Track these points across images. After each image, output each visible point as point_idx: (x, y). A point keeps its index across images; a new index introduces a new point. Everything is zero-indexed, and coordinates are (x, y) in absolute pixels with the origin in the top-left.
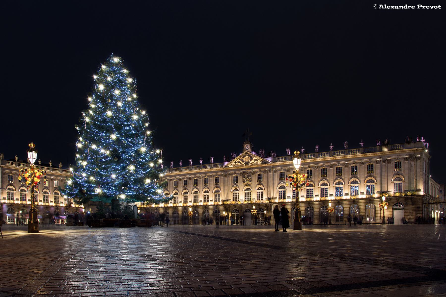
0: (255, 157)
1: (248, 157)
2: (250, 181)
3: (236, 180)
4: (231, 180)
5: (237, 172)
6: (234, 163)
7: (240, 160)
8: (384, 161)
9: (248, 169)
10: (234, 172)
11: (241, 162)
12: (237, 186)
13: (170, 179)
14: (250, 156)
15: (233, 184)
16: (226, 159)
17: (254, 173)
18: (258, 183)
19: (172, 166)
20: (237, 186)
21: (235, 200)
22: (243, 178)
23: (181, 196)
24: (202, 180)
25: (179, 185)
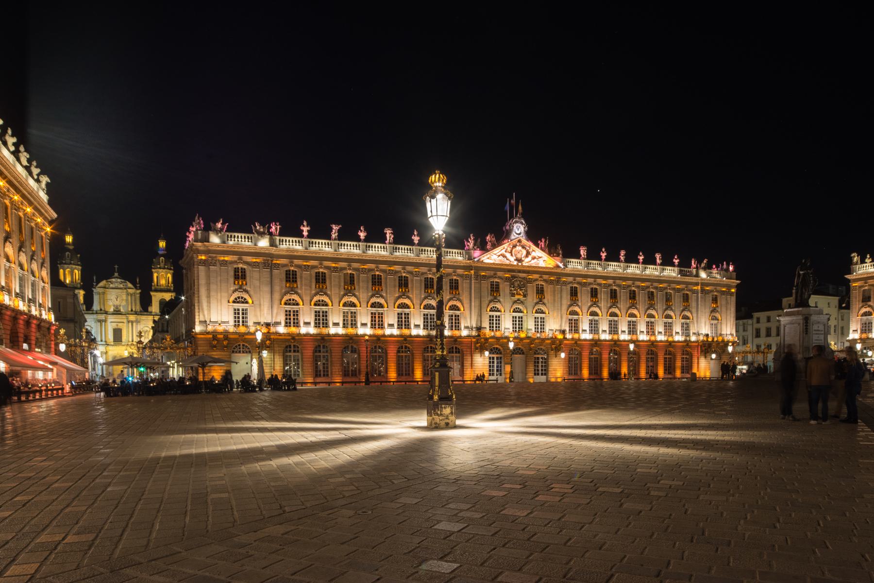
0: (533, 251)
1: (520, 248)
2: (525, 296)
3: (495, 289)
4: (488, 288)
5: (500, 274)
6: (495, 257)
7: (506, 251)
8: (703, 290)
9: (519, 271)
10: (492, 274)
11: (508, 255)
12: (499, 301)
13: (334, 267)
14: (523, 247)
15: (490, 298)
16: (475, 244)
17: (530, 281)
18: (538, 300)
19: (334, 235)
20: (499, 301)
21: (493, 330)
22: (510, 287)
23: (366, 312)
24: (421, 280)
25: (359, 285)
